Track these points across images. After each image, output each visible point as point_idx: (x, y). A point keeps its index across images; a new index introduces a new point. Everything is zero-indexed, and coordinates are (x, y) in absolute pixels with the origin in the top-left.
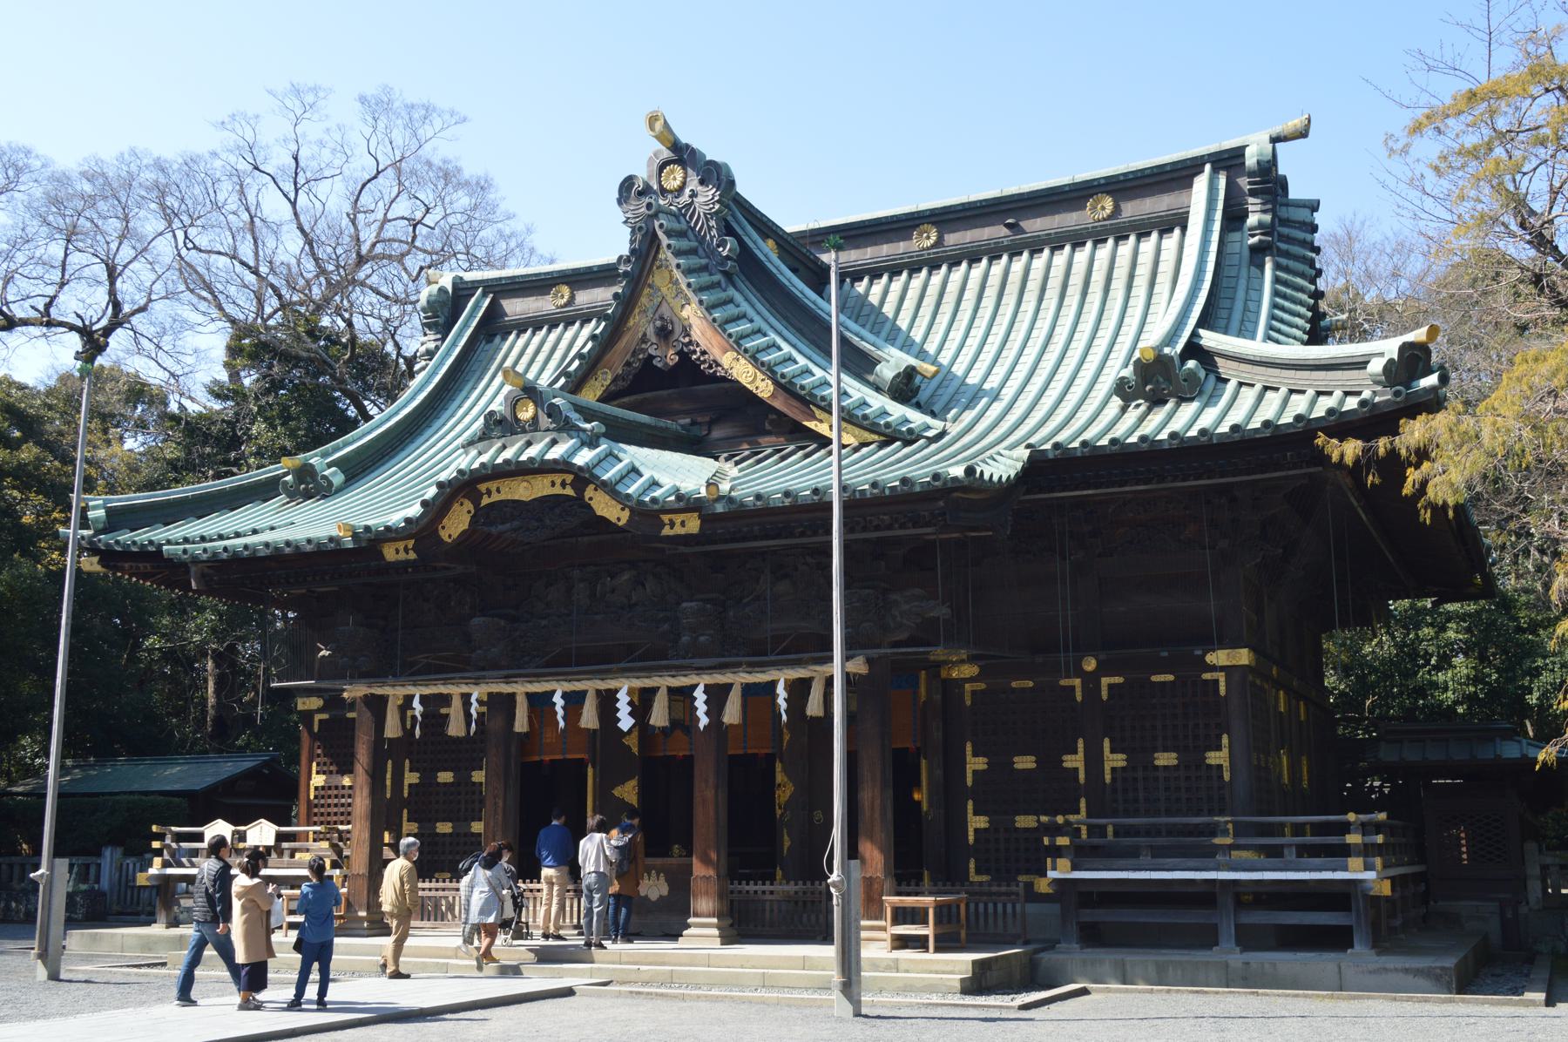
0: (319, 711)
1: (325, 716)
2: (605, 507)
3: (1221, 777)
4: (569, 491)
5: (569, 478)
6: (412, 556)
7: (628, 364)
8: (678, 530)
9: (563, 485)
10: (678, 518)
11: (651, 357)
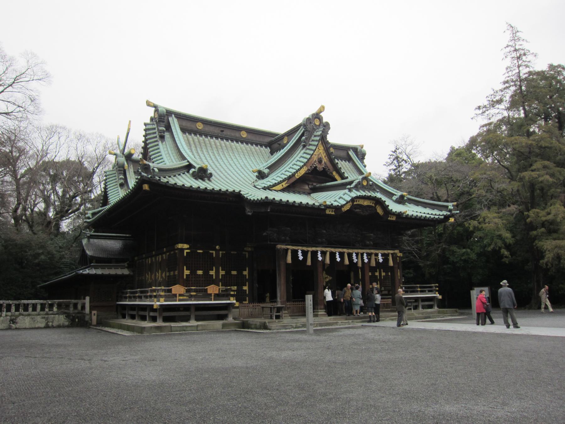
0: (187, 249)
2: (380, 211)
4: (373, 205)
6: (333, 213)
8: (391, 219)
11: (316, 167)
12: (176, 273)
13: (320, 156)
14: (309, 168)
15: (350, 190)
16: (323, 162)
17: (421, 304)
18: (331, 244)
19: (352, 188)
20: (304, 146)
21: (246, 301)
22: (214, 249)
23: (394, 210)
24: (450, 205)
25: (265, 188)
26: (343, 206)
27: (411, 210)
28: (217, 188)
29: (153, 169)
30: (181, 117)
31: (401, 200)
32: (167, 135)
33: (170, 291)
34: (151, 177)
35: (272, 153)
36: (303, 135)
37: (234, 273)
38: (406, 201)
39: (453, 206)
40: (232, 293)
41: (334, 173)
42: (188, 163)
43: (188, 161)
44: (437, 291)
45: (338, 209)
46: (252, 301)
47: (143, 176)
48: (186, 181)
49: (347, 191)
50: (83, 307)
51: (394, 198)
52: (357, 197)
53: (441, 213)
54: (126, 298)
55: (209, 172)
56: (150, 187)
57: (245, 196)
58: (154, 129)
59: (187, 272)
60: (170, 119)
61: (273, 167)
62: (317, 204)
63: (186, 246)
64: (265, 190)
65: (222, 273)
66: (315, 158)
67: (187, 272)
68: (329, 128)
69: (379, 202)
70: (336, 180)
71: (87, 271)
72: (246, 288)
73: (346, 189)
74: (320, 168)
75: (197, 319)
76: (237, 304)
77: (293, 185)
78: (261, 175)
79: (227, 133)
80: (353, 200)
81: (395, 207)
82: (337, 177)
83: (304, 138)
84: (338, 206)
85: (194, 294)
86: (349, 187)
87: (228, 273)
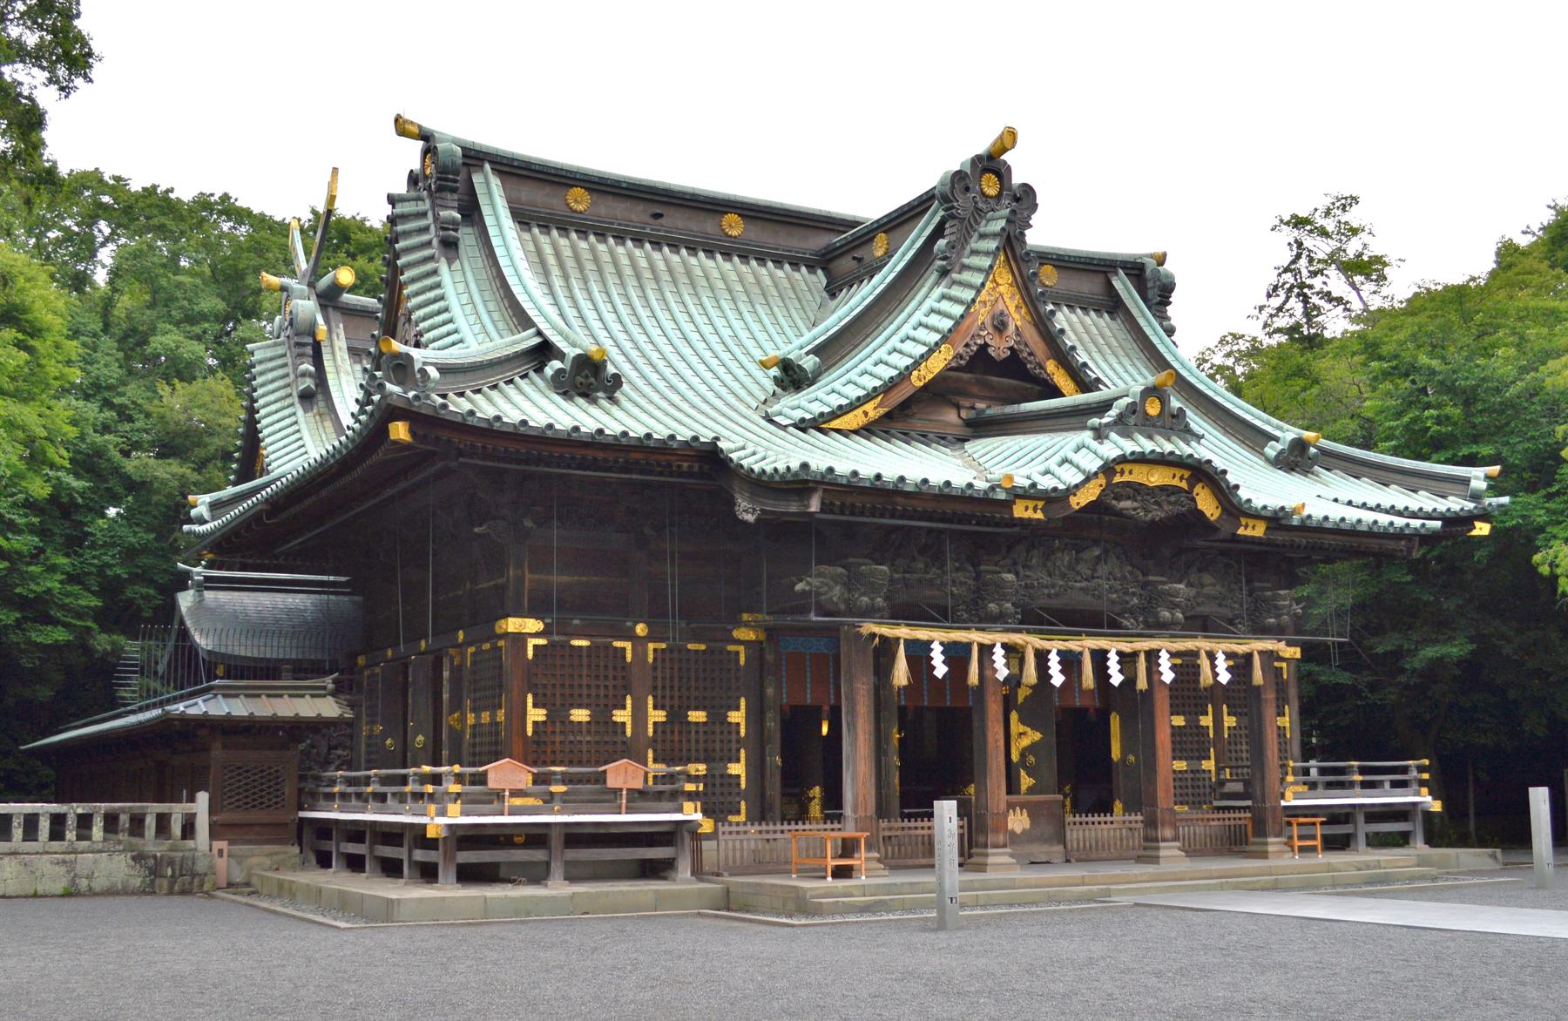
0: (536, 635)
1: (542, 642)
2: (1207, 504)
3: (738, 732)
4: (1184, 485)
5: (1187, 474)
6: (1039, 515)
7: (967, 345)
8: (1249, 532)
9: (1181, 478)
10: (1251, 522)
11: (986, 345)
12: (501, 715)
13: (1000, 306)
14: (961, 350)
15: (1100, 434)
16: (1011, 328)
17: (1363, 829)
18: (1032, 619)
19: (1107, 425)
20: (944, 273)
21: (738, 812)
22: (630, 636)
23: (1258, 503)
24: (1478, 477)
25: (802, 426)
26: (1072, 490)
27: (1327, 498)
28: (637, 431)
29: (423, 371)
30: (513, 169)
31: (1296, 460)
32: (467, 237)
33: (481, 779)
34: (417, 397)
35: (832, 291)
36: (938, 232)
37: (697, 716)
38: (1314, 460)
39: (1487, 477)
40: (690, 787)
41: (1051, 366)
42: (538, 340)
43: (539, 333)
44: (1422, 783)
45: (1055, 499)
46: (761, 814)
47: (391, 394)
48: (533, 406)
49: (1086, 436)
50: (189, 829)
51: (1271, 450)
52: (1123, 459)
53: (1442, 505)
54: (330, 797)
55: (611, 369)
56: (412, 432)
57: (734, 456)
58: (424, 215)
59: (536, 715)
60: (477, 179)
61: (833, 350)
62: (981, 485)
63: (533, 625)
64: (804, 430)
65: (656, 716)
66: (983, 314)
67: (536, 715)
68: (1034, 207)
69: (1202, 473)
70: (1056, 392)
71: (199, 707)
72: (737, 769)
73: (1084, 428)
74: (999, 348)
75: (571, 878)
76: (707, 826)
77: (902, 412)
78: (792, 377)
79: (676, 221)
80: (1108, 469)
81: (1263, 486)
82: (1061, 379)
83: (942, 243)
84: (1055, 489)
85: (563, 788)
86: (1095, 421)
87: (677, 717)
